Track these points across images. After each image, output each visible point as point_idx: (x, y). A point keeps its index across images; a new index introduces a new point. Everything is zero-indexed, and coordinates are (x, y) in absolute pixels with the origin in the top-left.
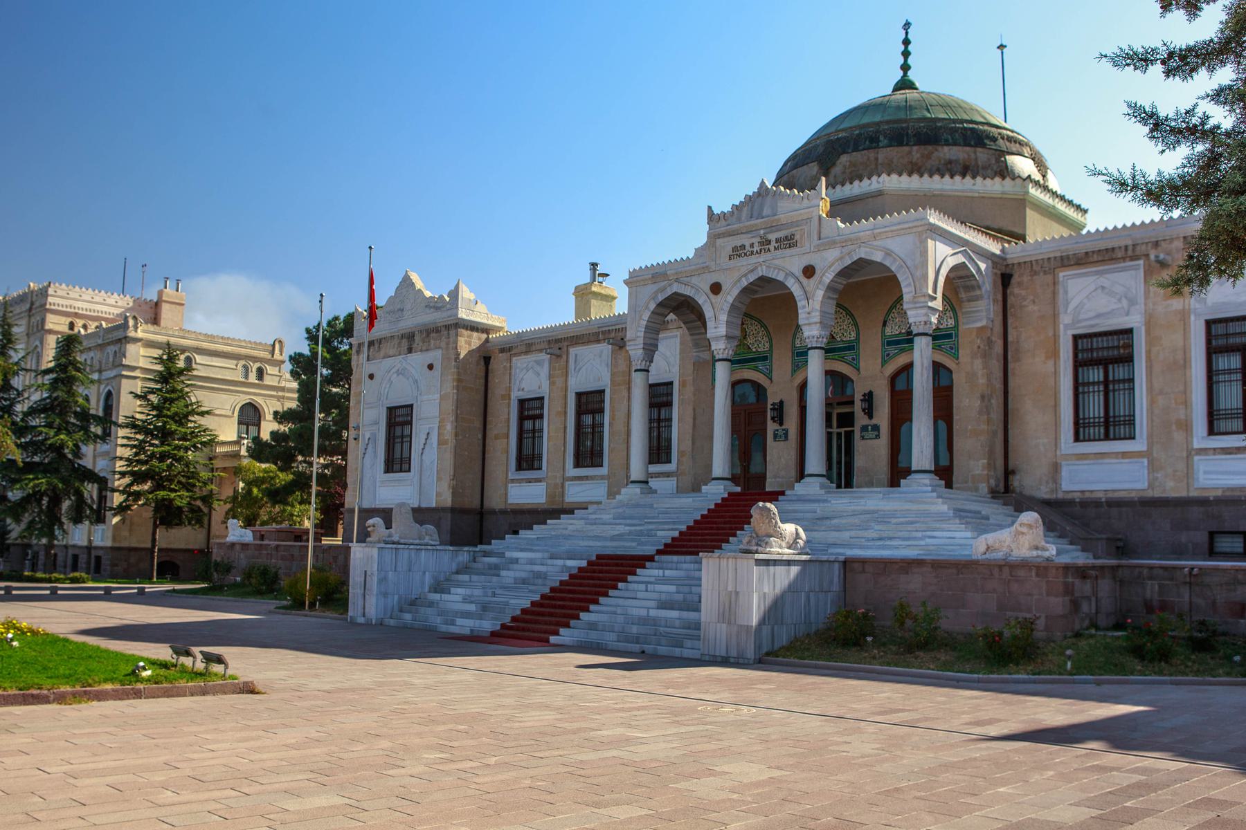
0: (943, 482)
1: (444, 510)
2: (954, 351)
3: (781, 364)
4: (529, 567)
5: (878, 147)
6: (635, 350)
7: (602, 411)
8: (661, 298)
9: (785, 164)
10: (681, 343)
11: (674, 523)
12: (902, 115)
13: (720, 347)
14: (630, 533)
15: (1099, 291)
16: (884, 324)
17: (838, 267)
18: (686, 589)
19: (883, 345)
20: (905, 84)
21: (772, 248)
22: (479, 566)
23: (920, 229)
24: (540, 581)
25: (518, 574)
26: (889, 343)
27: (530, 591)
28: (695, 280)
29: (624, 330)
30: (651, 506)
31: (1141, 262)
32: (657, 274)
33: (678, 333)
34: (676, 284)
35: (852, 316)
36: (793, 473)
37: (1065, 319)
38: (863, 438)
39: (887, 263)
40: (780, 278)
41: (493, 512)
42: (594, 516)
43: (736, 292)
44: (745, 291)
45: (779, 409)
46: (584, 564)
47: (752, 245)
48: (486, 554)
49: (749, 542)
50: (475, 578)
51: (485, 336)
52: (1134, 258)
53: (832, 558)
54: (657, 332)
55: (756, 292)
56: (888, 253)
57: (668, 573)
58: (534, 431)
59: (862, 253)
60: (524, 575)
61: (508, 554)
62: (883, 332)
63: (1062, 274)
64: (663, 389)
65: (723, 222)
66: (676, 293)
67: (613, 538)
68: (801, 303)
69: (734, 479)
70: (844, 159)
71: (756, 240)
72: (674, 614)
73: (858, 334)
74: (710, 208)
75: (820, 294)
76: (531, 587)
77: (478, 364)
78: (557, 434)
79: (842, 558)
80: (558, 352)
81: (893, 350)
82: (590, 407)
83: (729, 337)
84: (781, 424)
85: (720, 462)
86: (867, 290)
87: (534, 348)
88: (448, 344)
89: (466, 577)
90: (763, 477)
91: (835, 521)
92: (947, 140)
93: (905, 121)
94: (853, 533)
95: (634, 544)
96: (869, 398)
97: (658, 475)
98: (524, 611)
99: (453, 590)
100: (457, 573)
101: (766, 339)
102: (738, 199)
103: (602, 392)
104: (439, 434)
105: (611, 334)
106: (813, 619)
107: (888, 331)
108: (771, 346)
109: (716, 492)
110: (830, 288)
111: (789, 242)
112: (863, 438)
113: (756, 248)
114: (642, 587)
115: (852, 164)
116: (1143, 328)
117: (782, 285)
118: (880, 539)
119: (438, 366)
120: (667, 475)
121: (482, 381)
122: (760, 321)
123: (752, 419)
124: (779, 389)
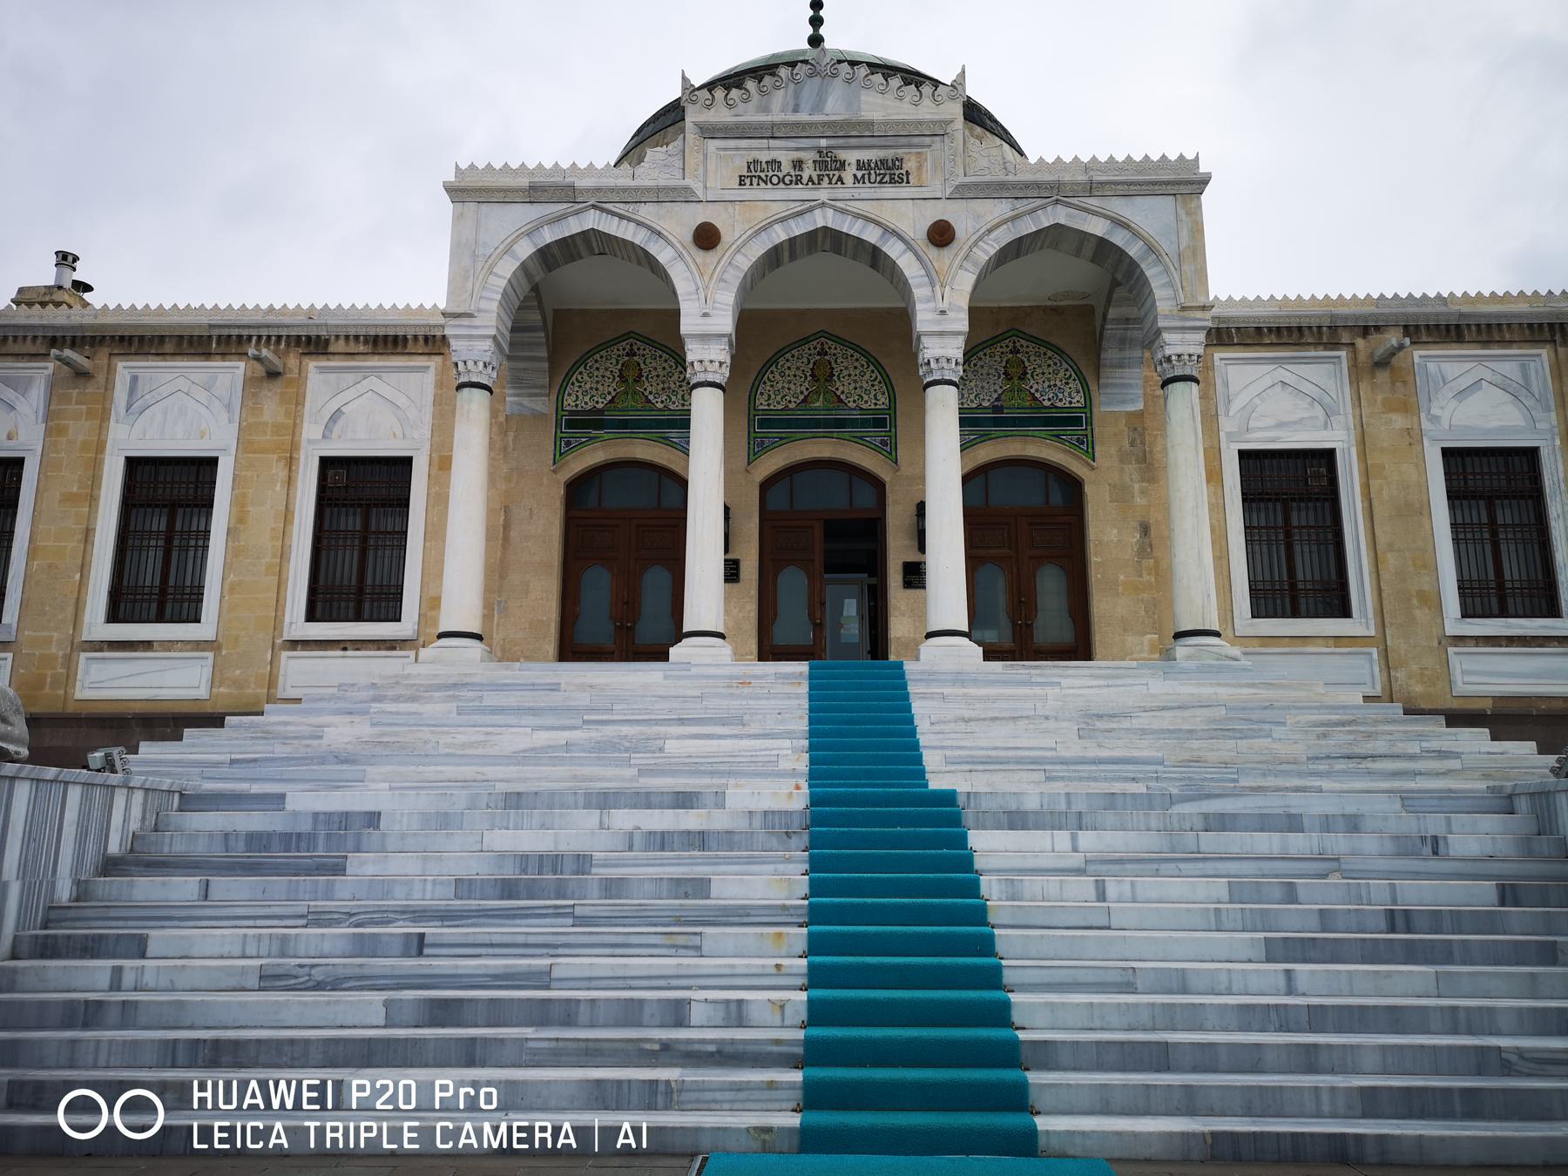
8: (549, 236)
14: (568, 746)
15: (1278, 388)
21: (848, 179)
28: (646, 212)
31: (1343, 353)
35: (879, 367)
47: (798, 164)
52: (1336, 345)
71: (809, 157)
73: (893, 400)
92: (810, 179)
116: (1354, 451)
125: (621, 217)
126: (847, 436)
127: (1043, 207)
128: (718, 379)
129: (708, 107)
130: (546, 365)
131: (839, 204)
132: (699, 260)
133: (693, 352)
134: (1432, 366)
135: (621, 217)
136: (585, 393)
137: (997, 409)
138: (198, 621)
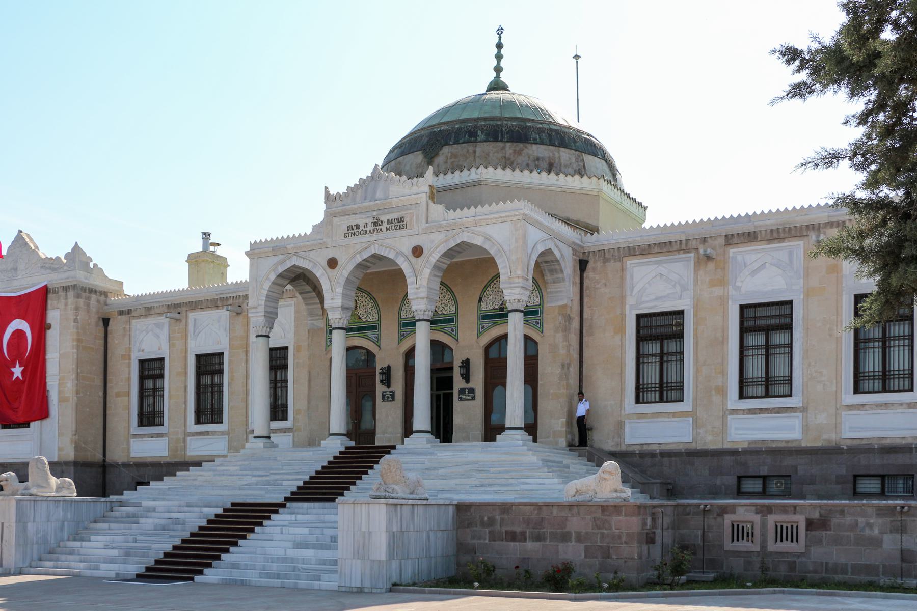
1: (66, 463)
2: (539, 326)
3: (389, 331)
4: (167, 515)
5: (476, 141)
6: (257, 318)
7: (221, 372)
8: (280, 270)
9: (392, 151)
10: (296, 312)
11: (298, 473)
12: (497, 113)
13: (336, 317)
15: (658, 278)
16: (480, 300)
17: (443, 249)
18: (318, 531)
19: (479, 319)
20: (497, 85)
22: (117, 514)
23: (515, 218)
24: (179, 527)
25: (157, 521)
26: (485, 317)
27: (171, 536)
28: (312, 255)
29: (246, 297)
30: (275, 459)
31: (692, 255)
32: (277, 247)
33: (293, 302)
34: (294, 258)
35: (452, 292)
36: (399, 429)
37: (630, 301)
38: (460, 399)
39: (486, 247)
40: (391, 256)
41: (116, 466)
42: (219, 468)
43: (351, 267)
44: (360, 266)
45: (387, 373)
46: (220, 511)
47: (366, 225)
48: (122, 504)
49: (378, 489)
50: (113, 525)
51: (102, 298)
52: (687, 251)
53: (447, 502)
54: (276, 301)
55: (369, 267)
56: (488, 238)
57: (299, 517)
58: (155, 390)
59: (465, 237)
60: (162, 521)
61: (145, 503)
62: (479, 307)
63: (630, 262)
64: (279, 354)
65: (339, 202)
66: (294, 266)
67: (241, 488)
68: (410, 280)
69: (348, 435)
70: (446, 150)
72: (309, 553)
73: (457, 309)
74: (326, 188)
75: (427, 272)
76: (172, 533)
77: (97, 325)
78: (179, 391)
79: (455, 502)
80: (178, 316)
81: (487, 323)
82: (209, 368)
83: (344, 308)
84: (389, 386)
85: (338, 420)
86: (468, 269)
87: (152, 312)
88: (66, 305)
89: (105, 525)
90: (372, 434)
91: (441, 471)
93: (500, 119)
94: (458, 481)
95: (263, 493)
96: (466, 364)
97: (276, 431)
98: (166, 555)
99: (92, 537)
100: (95, 522)
101: (375, 310)
102: (353, 182)
103: (221, 355)
104: (60, 392)
105: (233, 302)
106: (432, 555)
107: (483, 306)
108: (380, 317)
109: (334, 446)
110: (436, 267)
111: (399, 224)
112: (460, 399)
113: (369, 228)
114: (278, 530)
115: (454, 156)
117: (392, 262)
118: (482, 486)
120: (284, 431)
121: (102, 342)
122: (369, 294)
123: (363, 379)
124: (388, 354)
132: (330, 274)
134: (739, 258)
138: (222, 422)
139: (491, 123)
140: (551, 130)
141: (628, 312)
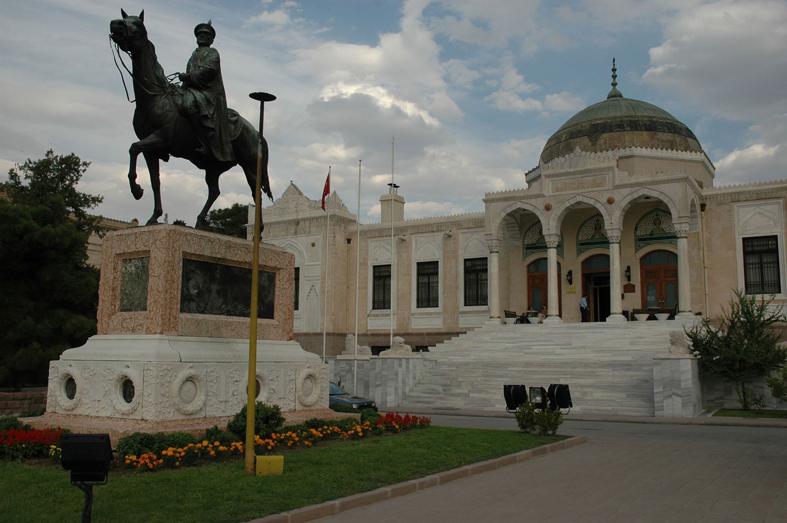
0: (626, 319)
8: (509, 210)
16: (636, 229)
26: (640, 240)
28: (533, 201)
62: (635, 233)
70: (605, 135)
81: (642, 243)
107: (638, 233)
119: (319, 244)
125: (527, 203)
126: (606, 246)
127: (640, 189)
128: (554, 246)
129: (547, 169)
130: (518, 232)
131: (582, 194)
133: (547, 239)
135: (527, 203)
136: (530, 239)
137: (652, 235)
139: (631, 119)
140: (667, 123)
141: (737, 236)
